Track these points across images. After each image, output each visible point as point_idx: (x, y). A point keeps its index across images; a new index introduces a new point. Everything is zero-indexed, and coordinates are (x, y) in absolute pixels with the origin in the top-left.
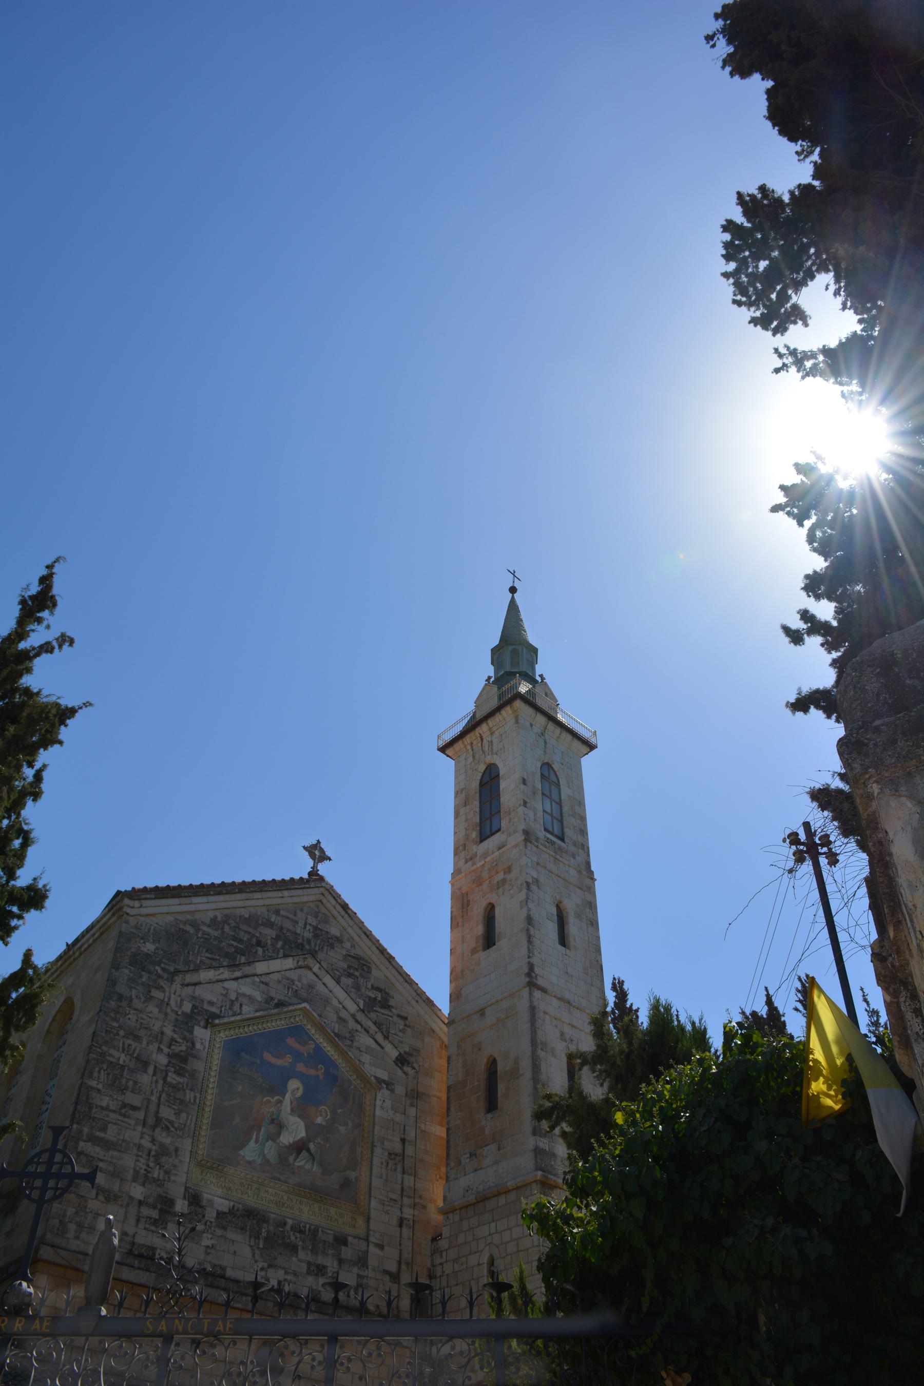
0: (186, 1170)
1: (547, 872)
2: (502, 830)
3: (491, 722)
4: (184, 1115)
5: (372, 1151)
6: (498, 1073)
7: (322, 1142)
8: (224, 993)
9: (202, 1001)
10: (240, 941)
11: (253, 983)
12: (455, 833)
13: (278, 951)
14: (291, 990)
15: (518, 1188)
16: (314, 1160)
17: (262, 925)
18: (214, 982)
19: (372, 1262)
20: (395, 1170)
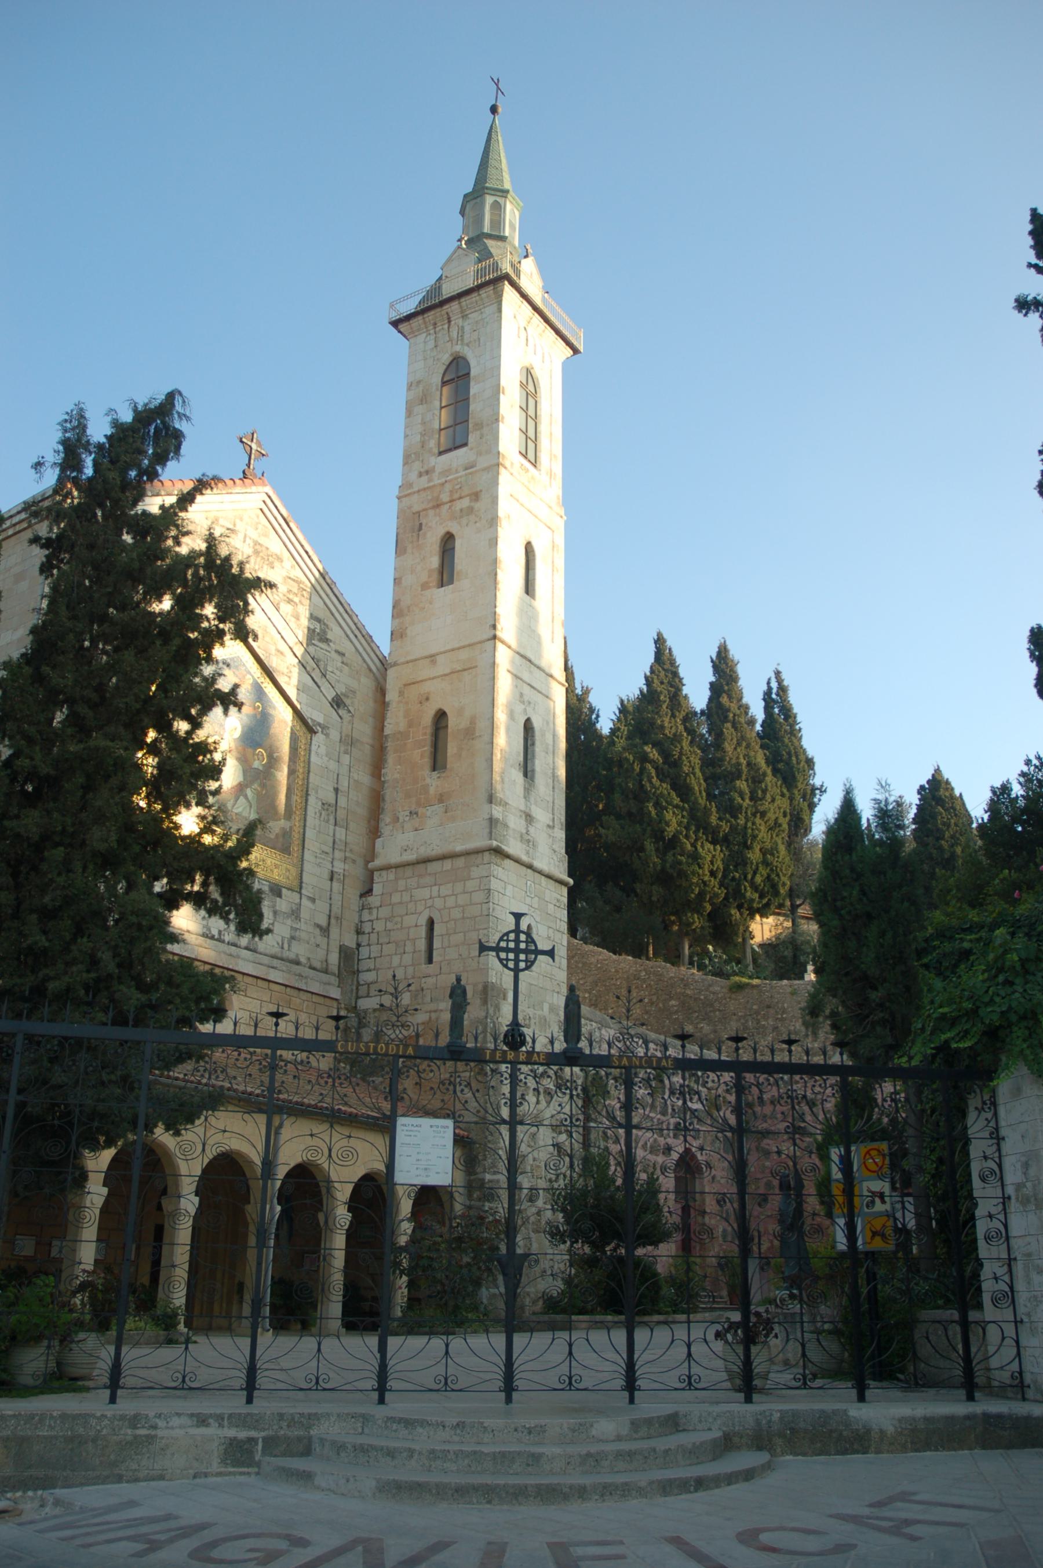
2: (470, 445)
3: (465, 301)
5: (307, 800)
6: (450, 730)
12: (406, 436)
15: (467, 853)
19: (304, 914)
20: (327, 821)
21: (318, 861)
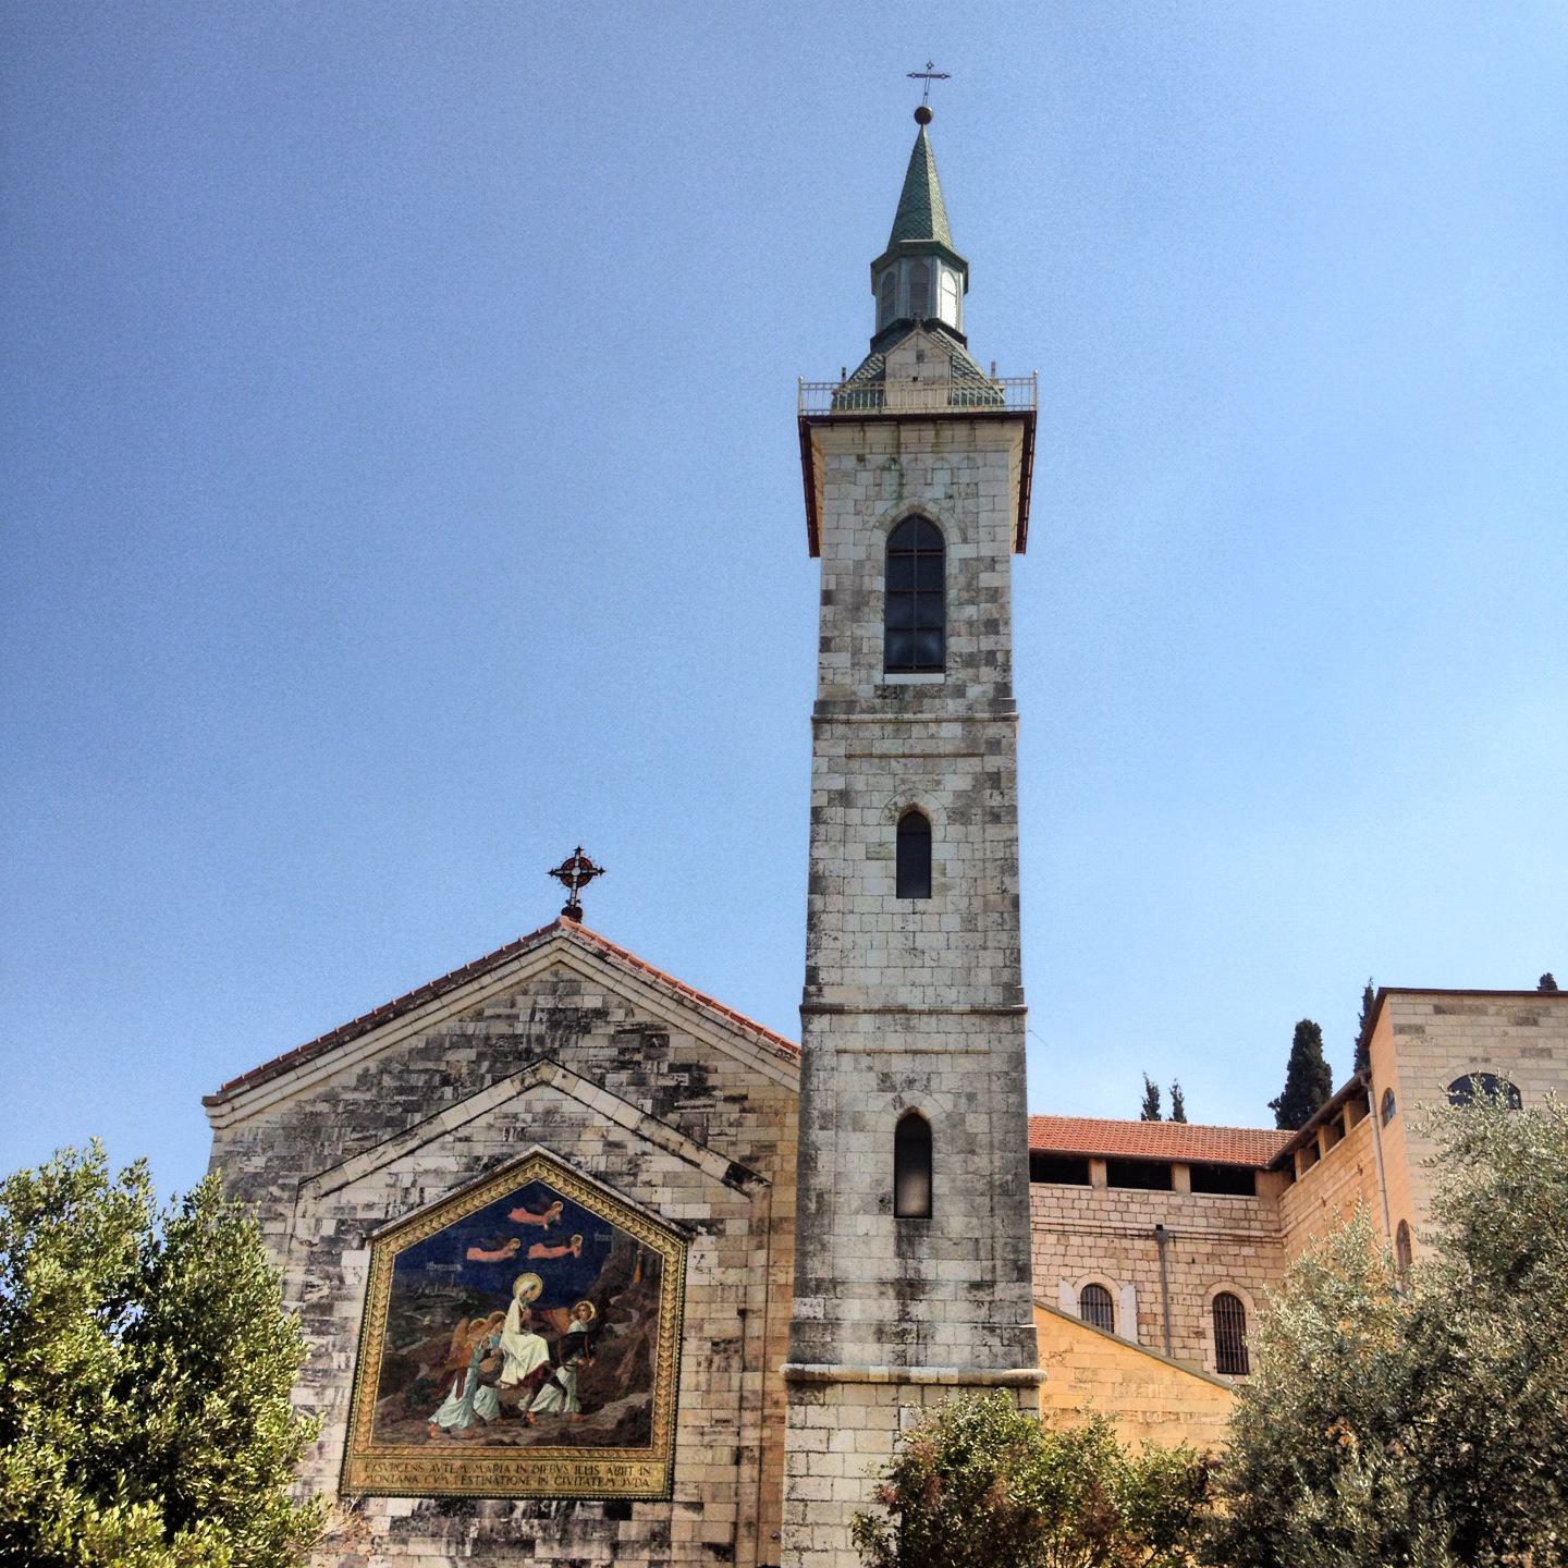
0: (337, 1470)
1: (876, 760)
4: (330, 1392)
7: (580, 1362)
8: (391, 1182)
9: (355, 1208)
10: (412, 1090)
11: (443, 1148)
13: (483, 1077)
14: (512, 1131)
16: (565, 1394)
17: (454, 1046)
18: (372, 1172)
19: (678, 1534)
20: (726, 1369)
21: (707, 1439)
